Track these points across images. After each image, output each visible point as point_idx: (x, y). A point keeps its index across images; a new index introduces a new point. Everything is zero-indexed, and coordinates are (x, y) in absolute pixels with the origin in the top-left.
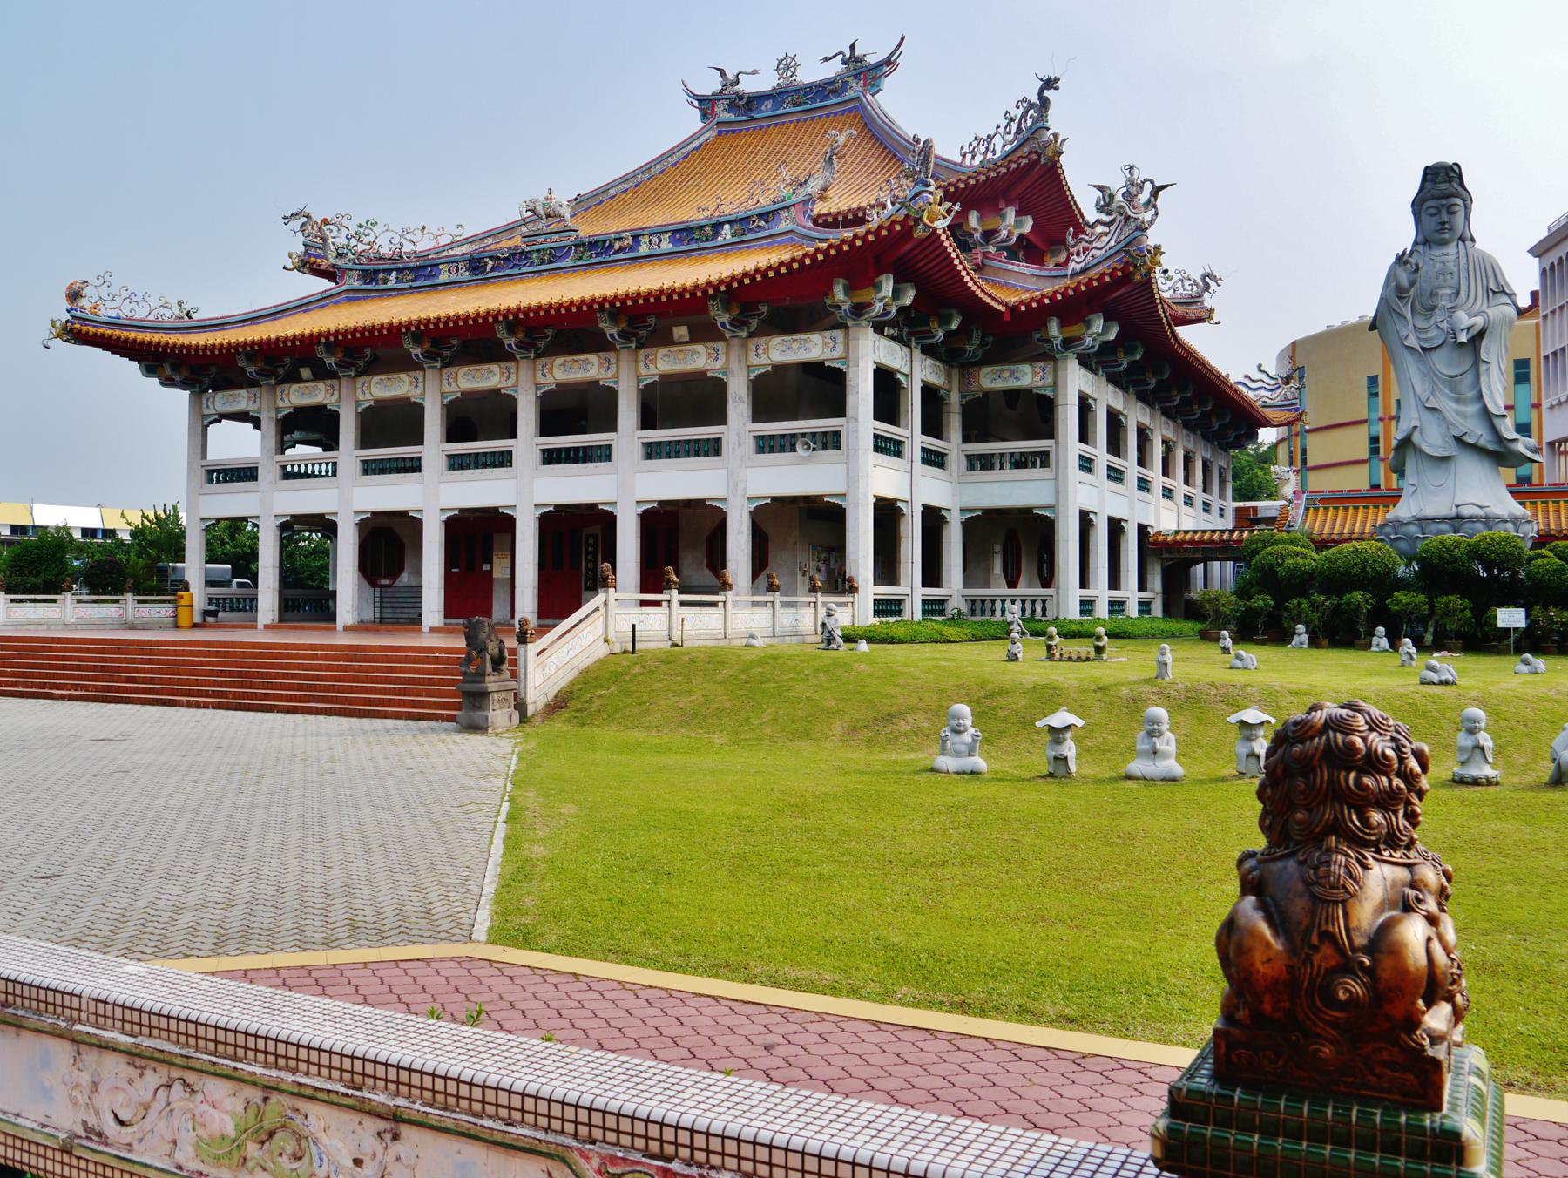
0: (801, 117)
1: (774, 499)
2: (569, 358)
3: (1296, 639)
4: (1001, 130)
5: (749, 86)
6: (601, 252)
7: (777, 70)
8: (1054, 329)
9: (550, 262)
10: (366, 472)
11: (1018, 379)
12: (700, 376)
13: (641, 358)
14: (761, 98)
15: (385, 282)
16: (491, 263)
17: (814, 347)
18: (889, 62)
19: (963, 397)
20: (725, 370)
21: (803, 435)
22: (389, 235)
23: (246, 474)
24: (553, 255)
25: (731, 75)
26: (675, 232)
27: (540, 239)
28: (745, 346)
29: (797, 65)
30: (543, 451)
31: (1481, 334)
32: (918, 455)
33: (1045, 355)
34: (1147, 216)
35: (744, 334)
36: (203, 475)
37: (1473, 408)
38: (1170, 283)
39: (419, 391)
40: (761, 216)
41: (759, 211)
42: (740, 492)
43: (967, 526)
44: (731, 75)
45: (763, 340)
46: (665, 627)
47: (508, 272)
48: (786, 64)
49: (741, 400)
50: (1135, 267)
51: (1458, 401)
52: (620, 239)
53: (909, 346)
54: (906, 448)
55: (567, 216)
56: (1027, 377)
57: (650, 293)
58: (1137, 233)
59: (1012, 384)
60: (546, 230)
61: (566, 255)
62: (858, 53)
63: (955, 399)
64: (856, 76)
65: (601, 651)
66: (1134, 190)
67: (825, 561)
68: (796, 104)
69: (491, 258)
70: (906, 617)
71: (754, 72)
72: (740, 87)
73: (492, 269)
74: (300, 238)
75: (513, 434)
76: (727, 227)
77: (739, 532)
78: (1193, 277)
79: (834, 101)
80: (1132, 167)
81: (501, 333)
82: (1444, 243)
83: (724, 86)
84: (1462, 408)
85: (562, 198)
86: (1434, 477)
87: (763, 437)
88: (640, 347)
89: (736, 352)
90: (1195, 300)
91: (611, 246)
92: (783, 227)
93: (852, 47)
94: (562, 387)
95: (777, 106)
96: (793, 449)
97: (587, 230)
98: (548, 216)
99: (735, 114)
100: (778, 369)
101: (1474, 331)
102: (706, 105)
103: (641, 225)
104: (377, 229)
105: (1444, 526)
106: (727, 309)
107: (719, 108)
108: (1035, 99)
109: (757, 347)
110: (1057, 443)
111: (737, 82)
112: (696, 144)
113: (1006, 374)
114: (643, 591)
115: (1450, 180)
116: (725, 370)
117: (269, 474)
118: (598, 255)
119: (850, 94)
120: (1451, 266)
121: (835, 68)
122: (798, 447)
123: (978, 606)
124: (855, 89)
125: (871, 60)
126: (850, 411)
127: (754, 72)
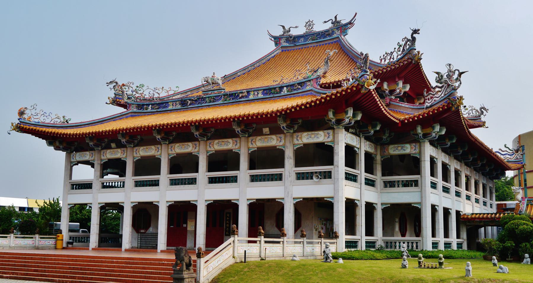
0: (315, 45)
1: (304, 199)
2: (220, 140)
3: (525, 260)
4: (396, 50)
5: (294, 32)
6: (234, 98)
7: (306, 26)
8: (419, 130)
9: (214, 102)
10: (172, 184)
11: (404, 150)
12: (274, 148)
13: (250, 140)
14: (299, 37)
15: (147, 109)
16: (189, 102)
17: (320, 137)
18: (351, 23)
19: (382, 157)
20: (284, 146)
21: (316, 172)
22: (149, 90)
23: (87, 186)
24: (215, 99)
25: (287, 28)
26: (264, 90)
27: (210, 92)
28: (292, 136)
29: (313, 24)
30: (209, 178)
32: (363, 181)
33: (416, 140)
34: (457, 84)
35: (292, 131)
36: (69, 186)
38: (467, 111)
39: (159, 153)
40: (299, 84)
41: (298, 82)
42: (290, 196)
43: (384, 211)
44: (287, 28)
45: (300, 134)
46: (258, 251)
47: (196, 106)
48: (309, 24)
49: (290, 158)
50: (452, 105)
52: (242, 93)
53: (359, 136)
54: (359, 179)
55: (221, 83)
56: (408, 149)
57: (254, 115)
58: (453, 91)
59: (402, 152)
60: (212, 89)
61: (220, 99)
62: (338, 19)
63: (378, 158)
64: (337, 29)
65: (231, 261)
66: (451, 74)
67: (325, 225)
68: (313, 40)
69: (190, 100)
70: (359, 248)
71: (296, 27)
72: (291, 33)
73: (190, 105)
74: (113, 91)
75: (197, 171)
76: (285, 88)
77: (290, 212)
78: (476, 109)
79: (329, 38)
80: (450, 65)
81: (193, 130)
83: (284, 33)
85: (219, 76)
87: (299, 173)
88: (249, 136)
89: (288, 139)
90: (478, 118)
91: (238, 96)
92: (308, 88)
93: (336, 17)
94: (218, 152)
95: (306, 40)
96: (312, 178)
97: (229, 89)
98: (213, 83)
99: (289, 44)
100: (305, 145)
102: (277, 40)
103: (250, 87)
104: (144, 88)
106: (285, 121)
107: (282, 41)
108: (410, 38)
109: (297, 137)
110: (421, 177)
111: (290, 31)
112: (273, 55)
113: (400, 148)
114: (250, 236)
116: (284, 146)
117: (97, 186)
118: (233, 99)
119: (335, 36)
121: (329, 25)
122: (314, 178)
123: (389, 244)
124: (337, 33)
125: (343, 22)
126: (335, 163)
127: (296, 27)
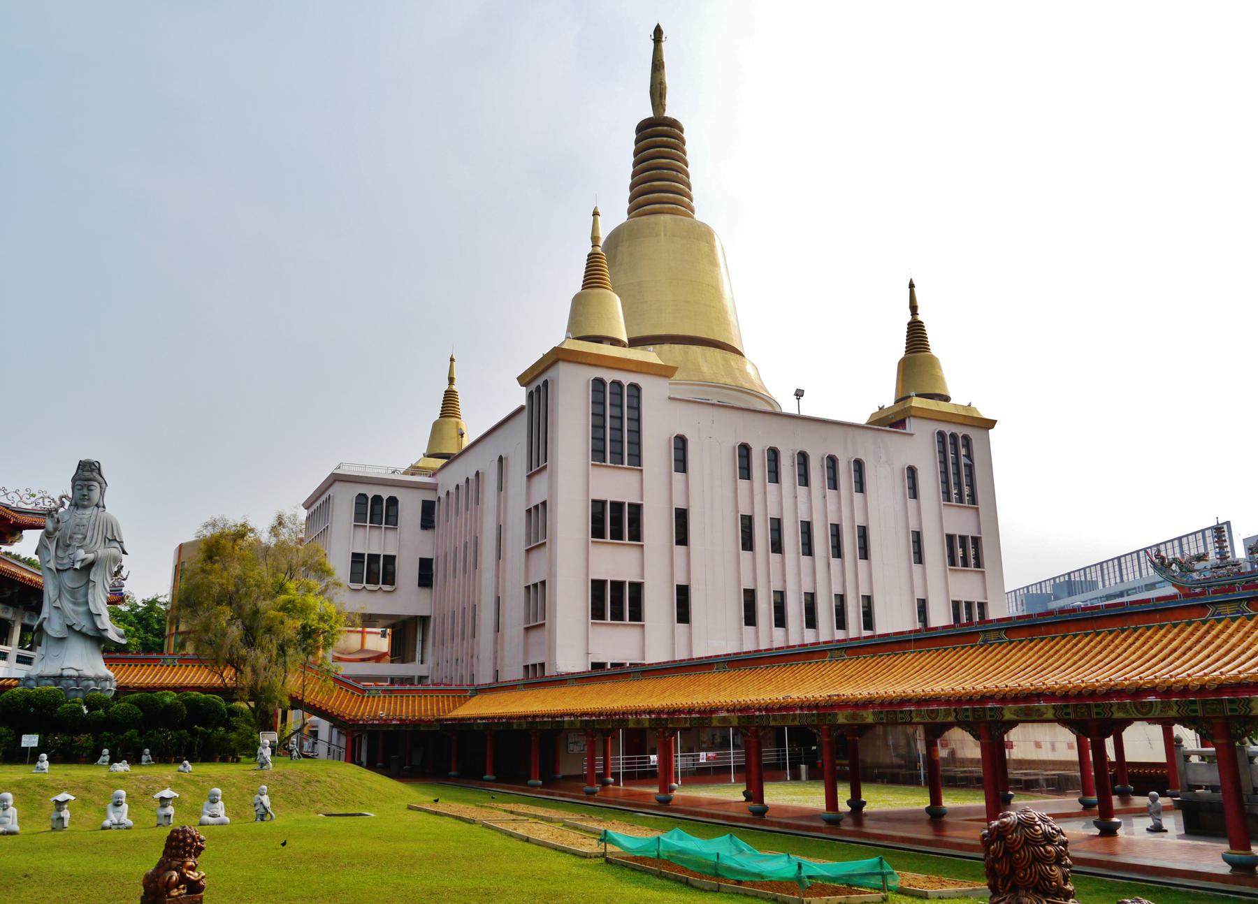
31: (92, 564)
37: (82, 609)
38: (33, 499)
51: (74, 604)
82: (85, 507)
84: (76, 608)
86: (54, 650)
101: (86, 562)
105: (49, 682)
115: (92, 471)
120: (85, 522)
